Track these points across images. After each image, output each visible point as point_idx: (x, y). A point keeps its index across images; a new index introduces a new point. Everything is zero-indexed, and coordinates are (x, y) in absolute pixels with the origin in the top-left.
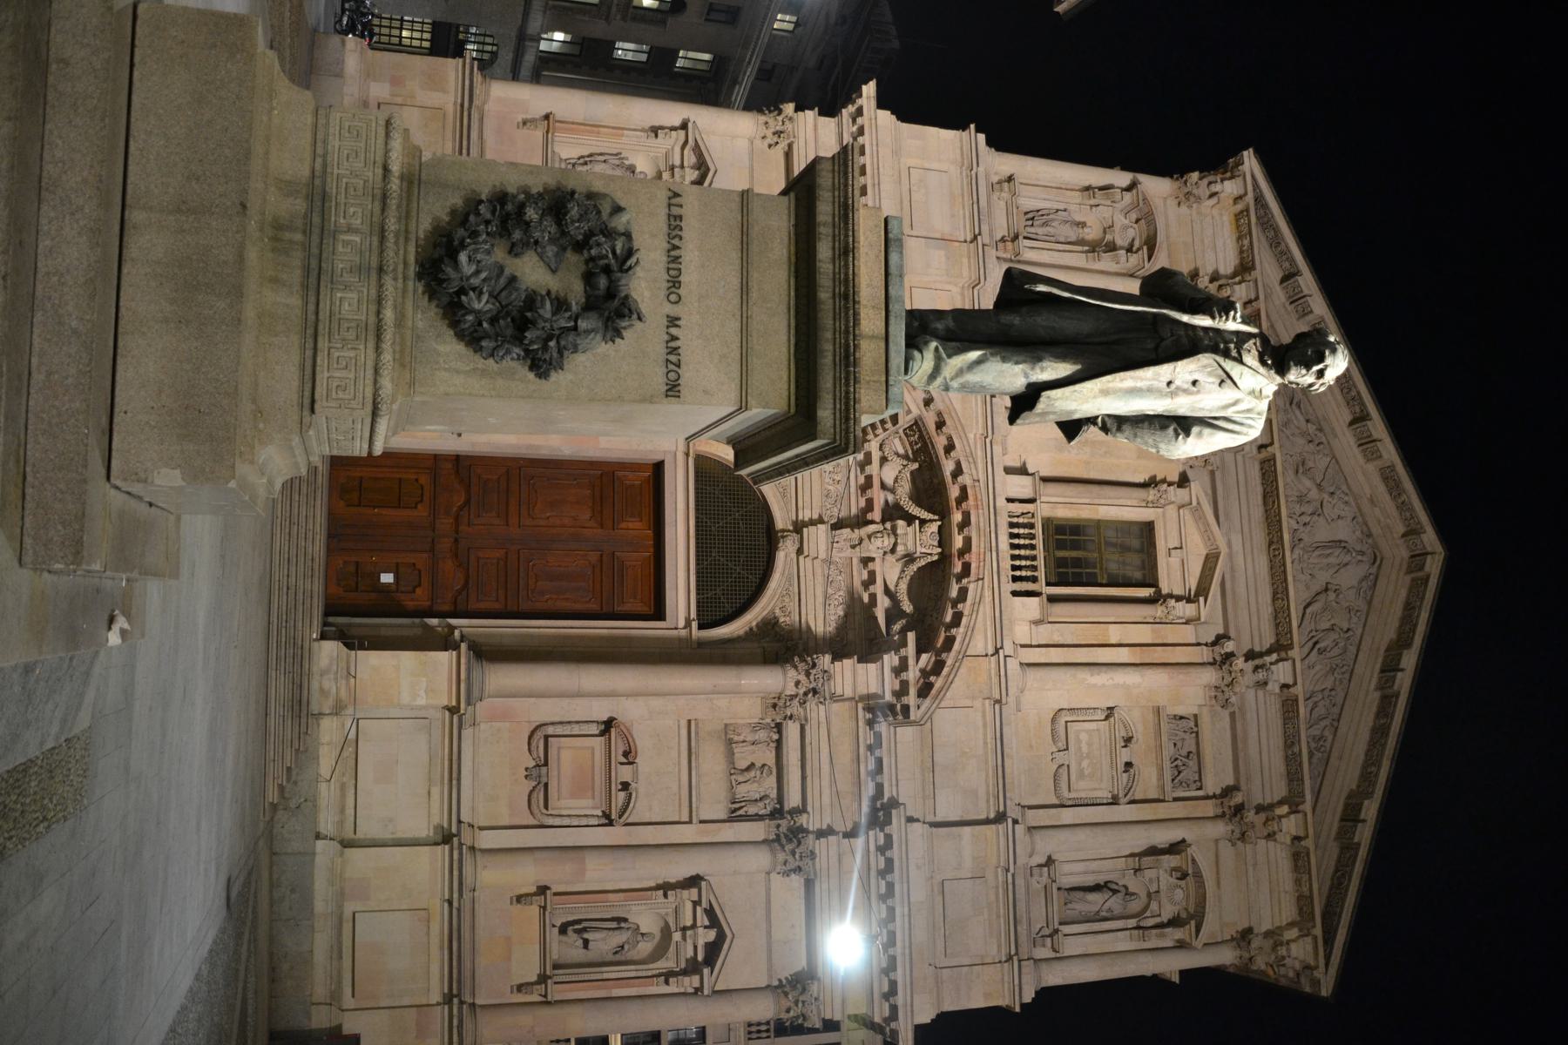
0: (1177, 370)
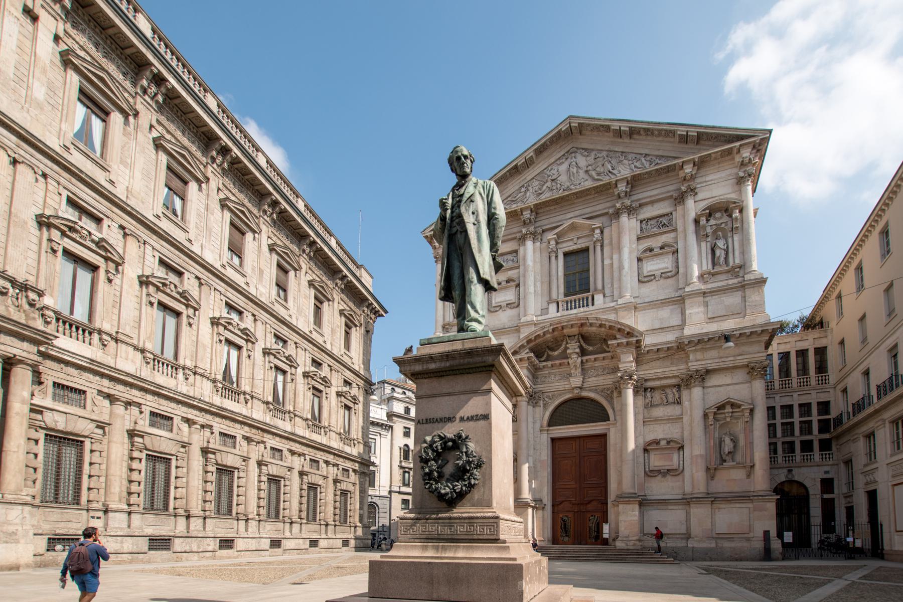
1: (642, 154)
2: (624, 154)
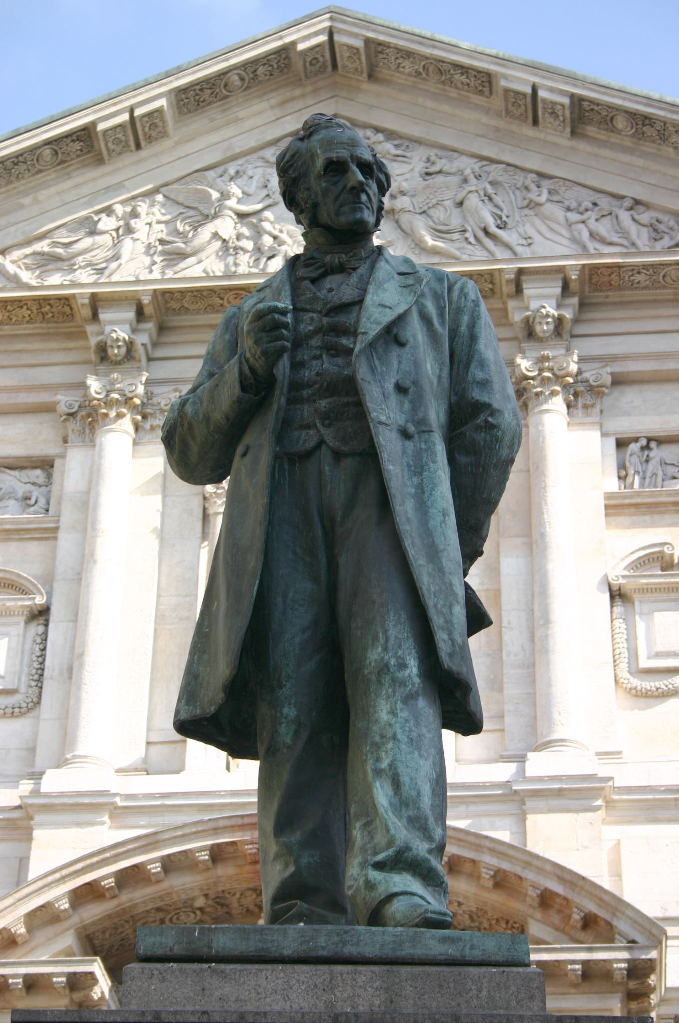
0: (383, 418)
1: (621, 197)
2: (546, 183)
